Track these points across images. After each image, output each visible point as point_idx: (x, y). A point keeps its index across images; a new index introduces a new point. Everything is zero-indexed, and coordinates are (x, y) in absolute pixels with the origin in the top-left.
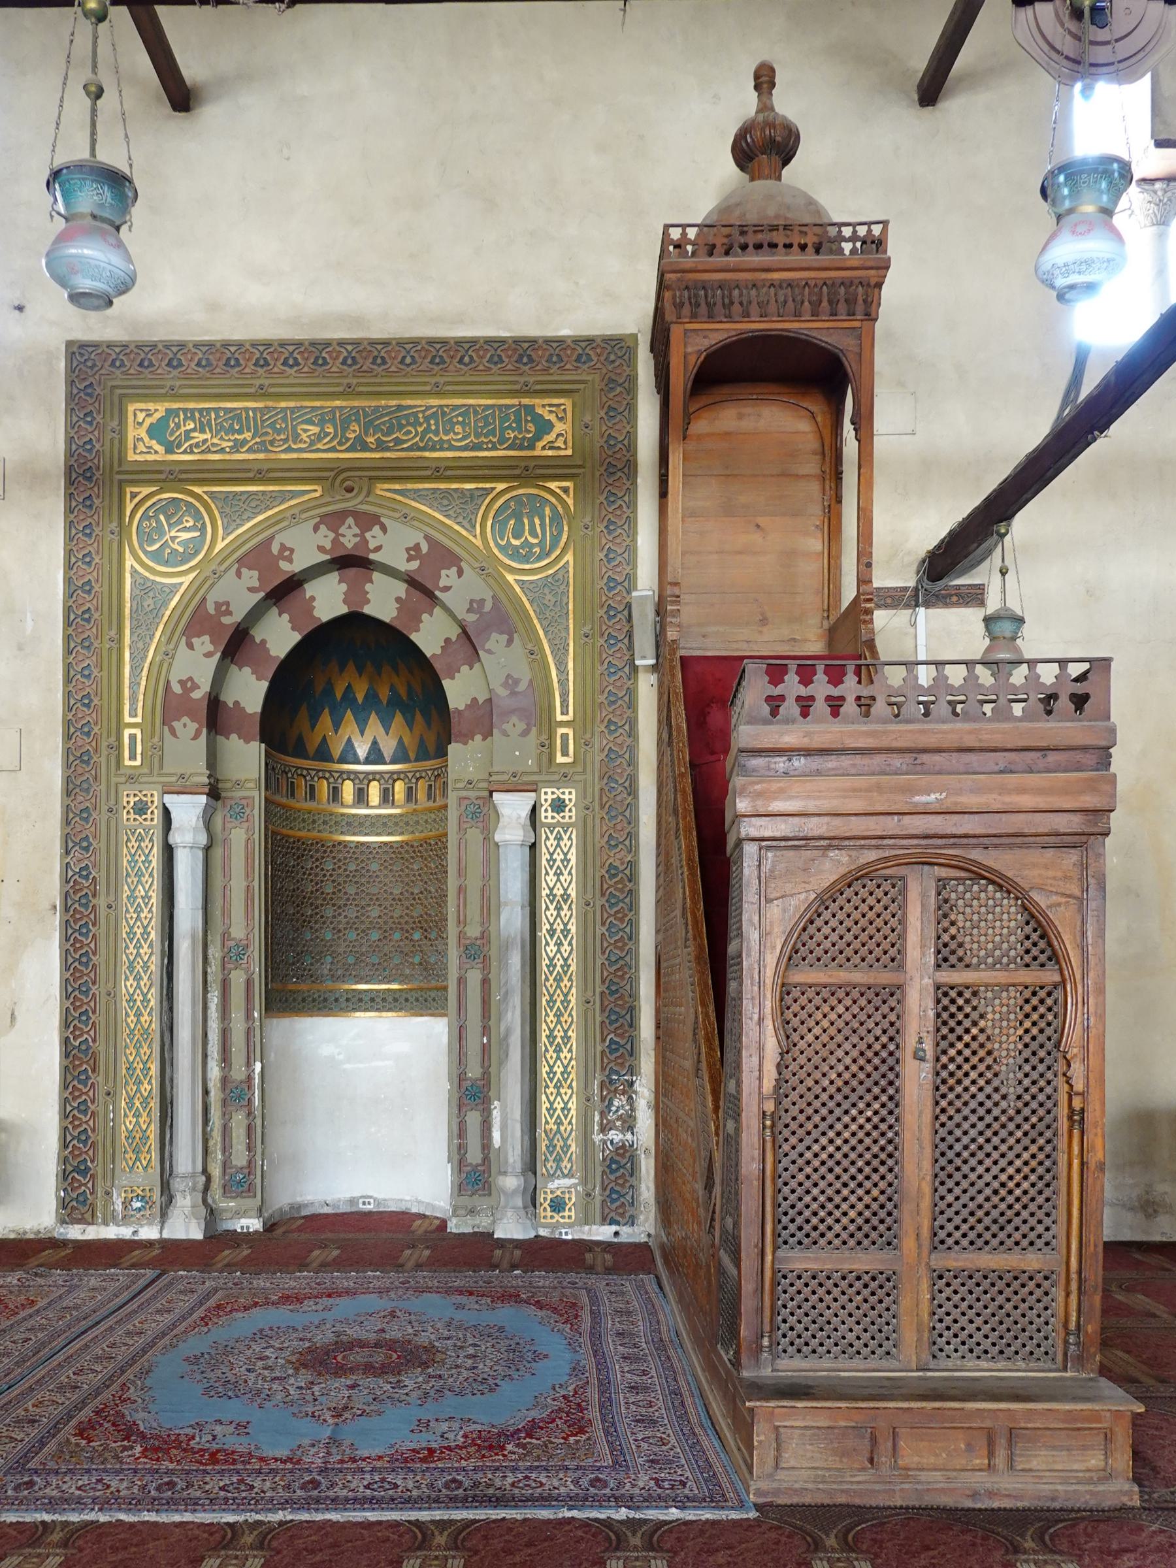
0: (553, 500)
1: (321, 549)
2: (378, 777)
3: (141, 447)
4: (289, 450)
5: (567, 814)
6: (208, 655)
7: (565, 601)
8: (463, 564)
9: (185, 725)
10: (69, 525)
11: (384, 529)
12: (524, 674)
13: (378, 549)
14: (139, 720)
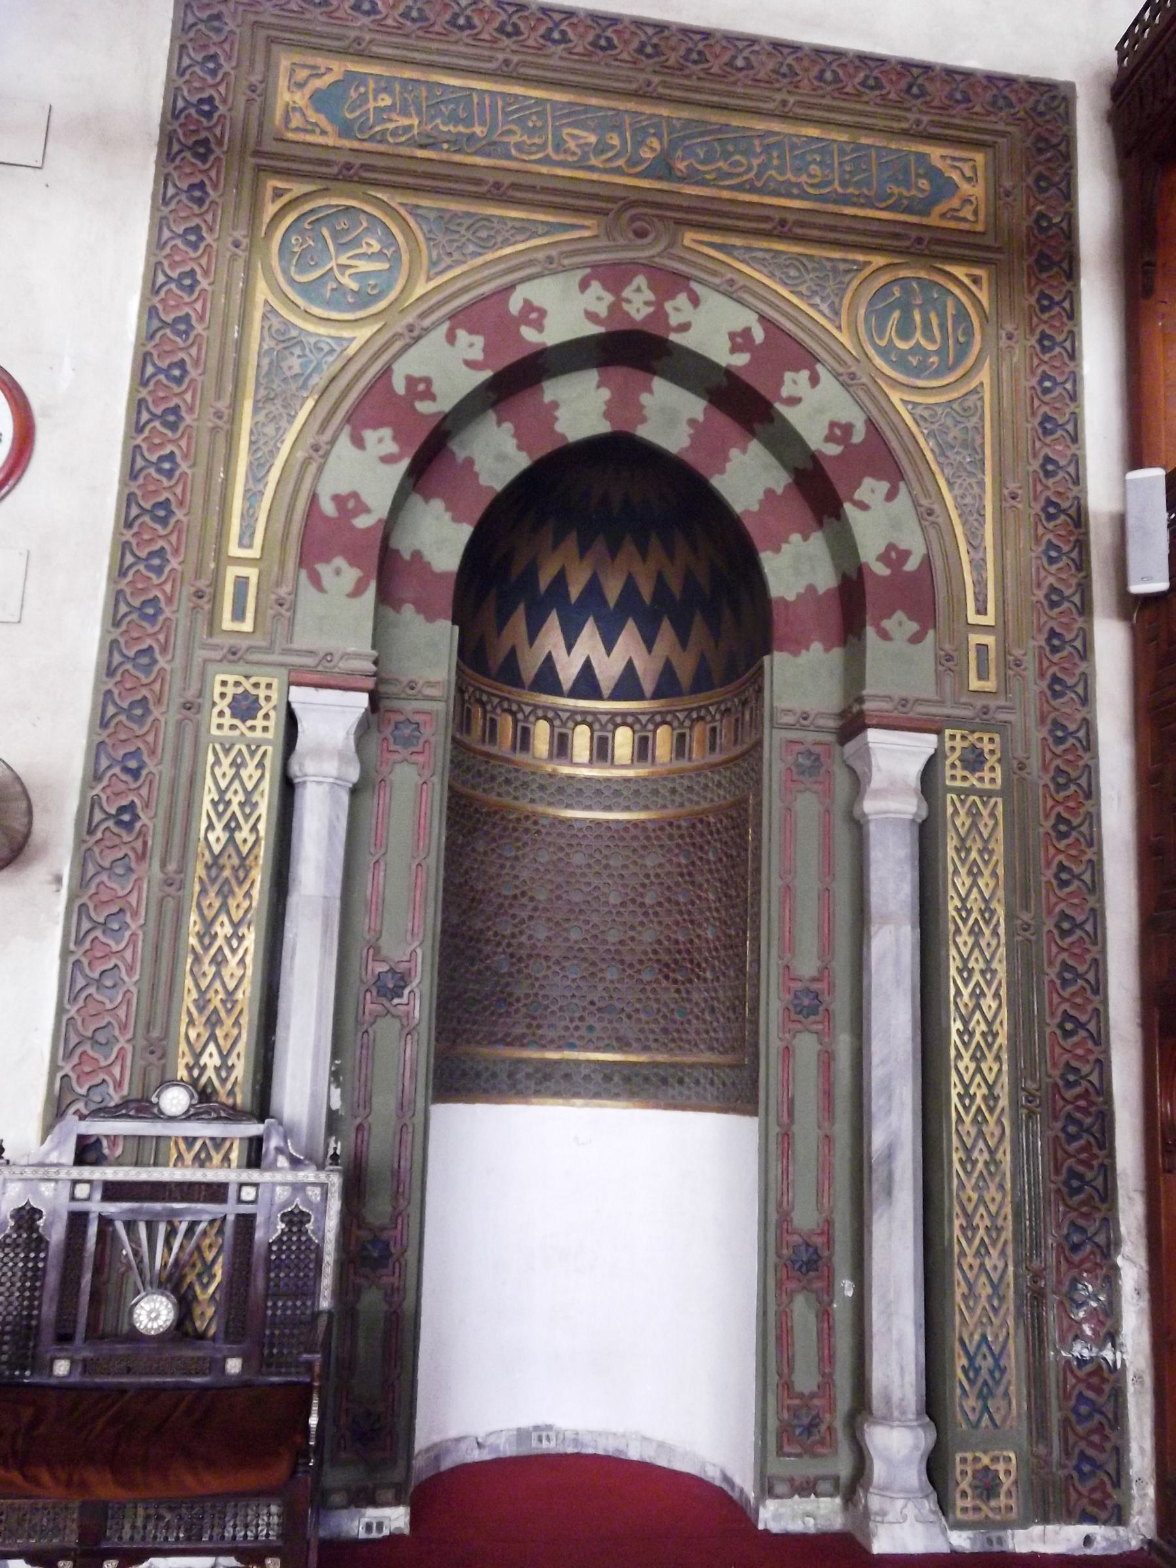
0: (957, 291)
1: (592, 316)
2: (590, 719)
3: (297, 120)
4: (546, 161)
5: (987, 775)
6: (388, 459)
7: (978, 442)
8: (819, 368)
9: (338, 572)
10: (158, 224)
11: (695, 301)
12: (914, 544)
13: (684, 327)
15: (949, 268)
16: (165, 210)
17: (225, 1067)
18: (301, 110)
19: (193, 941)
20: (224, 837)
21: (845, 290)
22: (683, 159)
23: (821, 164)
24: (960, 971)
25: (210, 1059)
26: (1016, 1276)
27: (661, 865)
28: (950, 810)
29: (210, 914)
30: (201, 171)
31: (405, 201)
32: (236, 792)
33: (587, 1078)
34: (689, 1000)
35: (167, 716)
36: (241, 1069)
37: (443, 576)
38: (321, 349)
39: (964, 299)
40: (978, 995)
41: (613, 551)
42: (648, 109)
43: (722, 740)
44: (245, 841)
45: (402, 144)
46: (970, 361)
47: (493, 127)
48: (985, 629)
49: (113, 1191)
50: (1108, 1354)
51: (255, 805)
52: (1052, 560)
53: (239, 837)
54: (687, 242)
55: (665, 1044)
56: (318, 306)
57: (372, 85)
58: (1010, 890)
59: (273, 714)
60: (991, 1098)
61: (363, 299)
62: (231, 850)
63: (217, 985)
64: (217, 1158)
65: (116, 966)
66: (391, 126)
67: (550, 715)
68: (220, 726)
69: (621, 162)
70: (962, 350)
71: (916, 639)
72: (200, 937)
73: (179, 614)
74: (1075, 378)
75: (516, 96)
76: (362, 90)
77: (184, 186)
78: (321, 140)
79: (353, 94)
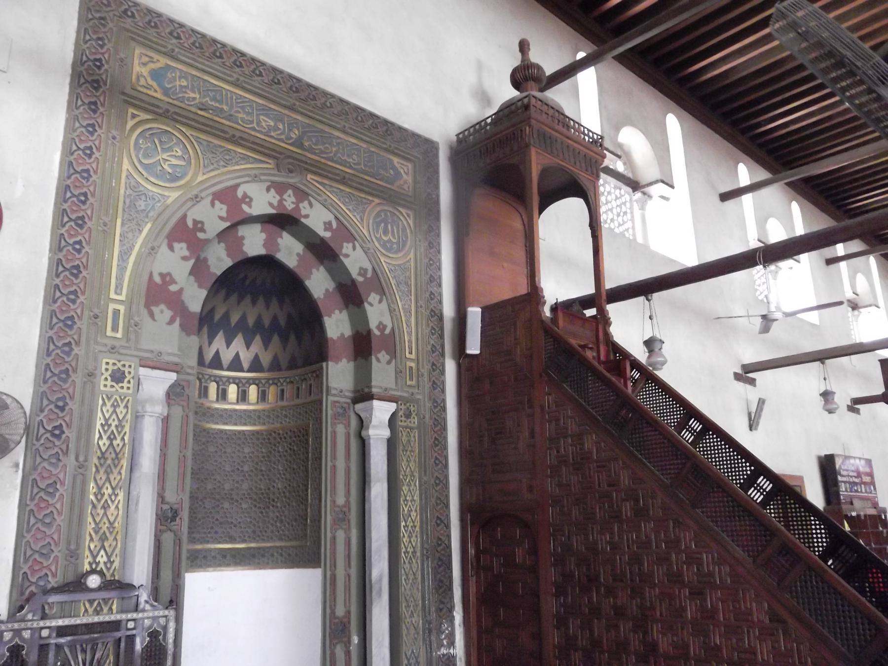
1: (271, 205)
3: (142, 82)
6: (185, 258)
9: (162, 312)
14: (122, 298)
15: (400, 209)
16: (77, 112)
18: (144, 77)
19: (92, 497)
20: (107, 443)
21: (365, 211)
22: (308, 141)
23: (357, 155)
24: (404, 501)
25: (102, 558)
26: (423, 623)
27: (253, 453)
28: (400, 434)
29: (100, 483)
30: (96, 96)
31: (193, 134)
32: (114, 420)
33: (214, 557)
34: (268, 517)
35: (78, 378)
37: (195, 313)
38: (154, 199)
39: (405, 223)
41: (241, 299)
42: (294, 116)
43: (287, 395)
44: (118, 445)
45: (191, 105)
47: (231, 107)
49: (62, 631)
50: (451, 651)
51: (123, 427)
52: (433, 334)
53: (115, 443)
54: (308, 179)
55: (255, 539)
56: (153, 177)
57: (178, 74)
58: (420, 468)
59: (132, 381)
60: (414, 552)
62: (111, 450)
63: (105, 520)
64: (106, 609)
65: (52, 512)
66: (187, 96)
67: (218, 379)
68: (105, 386)
69: (283, 137)
70: (404, 245)
71: (389, 363)
72: (95, 495)
73: (83, 324)
74: (439, 260)
75: (241, 96)
76: (174, 75)
77: (87, 101)
78: (155, 95)
79: (169, 75)
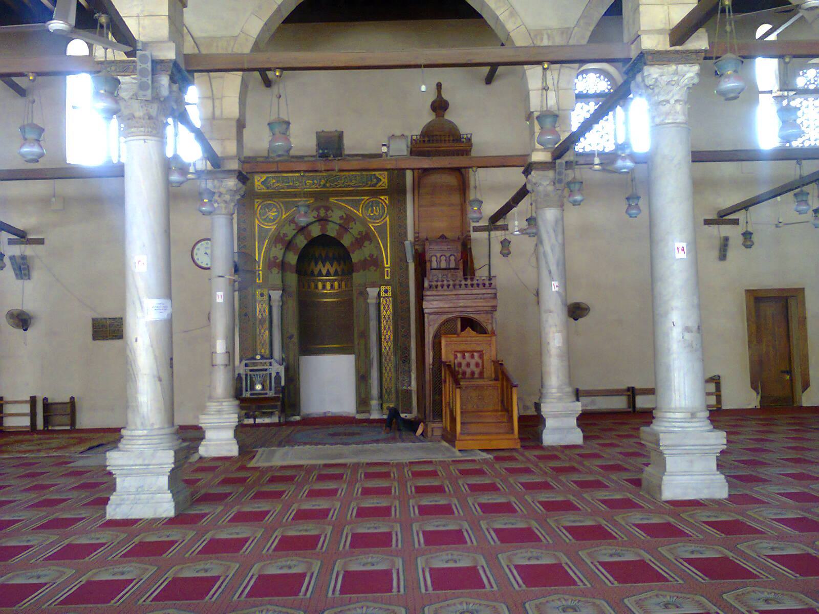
1: (314, 217)
11: (332, 211)
12: (375, 254)
17: (265, 352)
25: (263, 351)
36: (268, 352)
40: (387, 332)
46: (384, 216)
48: (388, 267)
49: (251, 370)
61: (274, 220)
74: (406, 216)
